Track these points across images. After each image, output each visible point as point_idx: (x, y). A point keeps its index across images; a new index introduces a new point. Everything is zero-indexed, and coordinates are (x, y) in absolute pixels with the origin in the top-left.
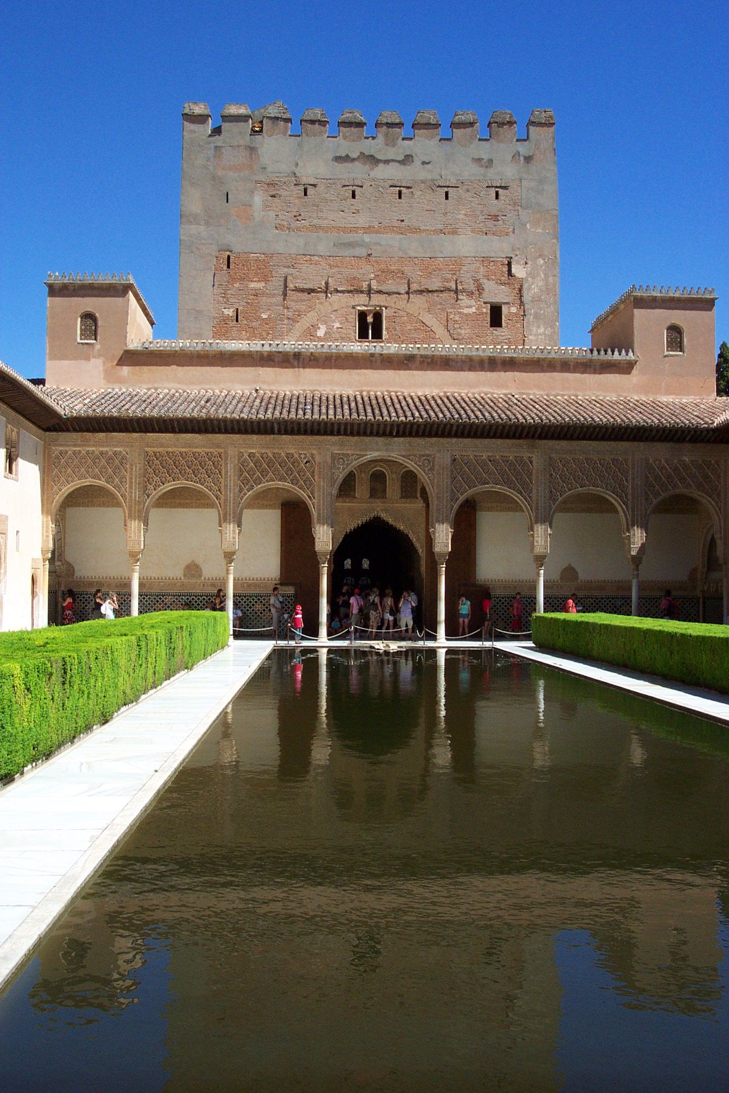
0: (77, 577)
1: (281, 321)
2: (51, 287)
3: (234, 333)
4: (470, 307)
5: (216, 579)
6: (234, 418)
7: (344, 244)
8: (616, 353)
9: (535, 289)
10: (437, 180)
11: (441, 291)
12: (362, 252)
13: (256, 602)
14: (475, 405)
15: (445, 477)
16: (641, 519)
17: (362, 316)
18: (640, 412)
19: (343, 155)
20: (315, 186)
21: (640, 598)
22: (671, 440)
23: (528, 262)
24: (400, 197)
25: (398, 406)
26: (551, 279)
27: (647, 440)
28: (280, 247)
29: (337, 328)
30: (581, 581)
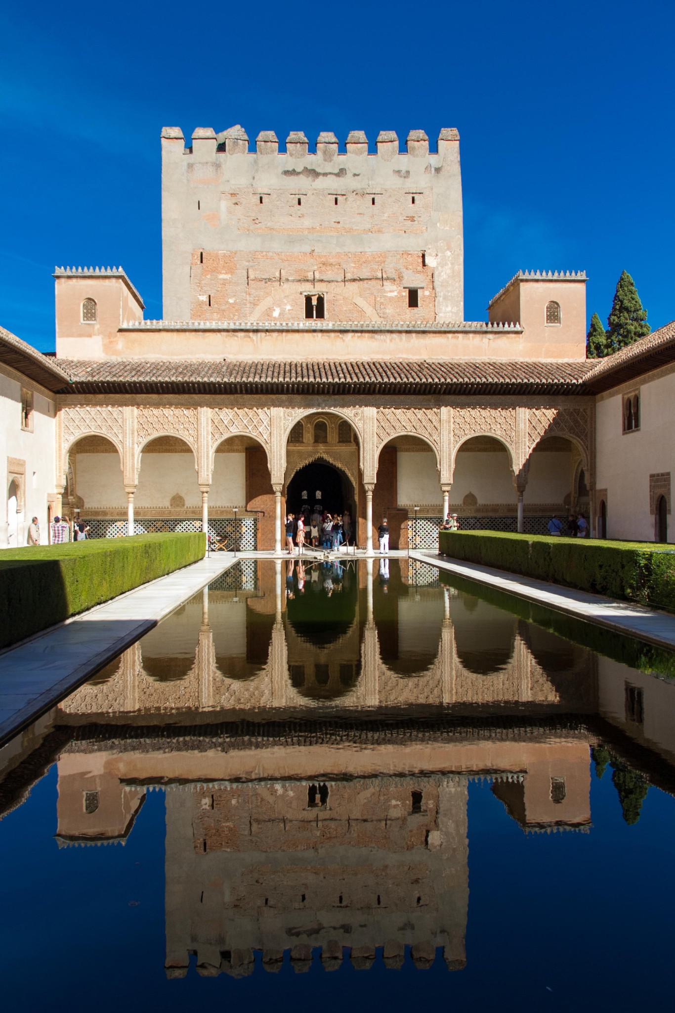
0: (86, 508)
5: (196, 507)
6: (205, 381)
8: (506, 325)
9: (444, 276)
10: (365, 189)
11: (370, 279)
12: (307, 249)
13: (227, 525)
14: (394, 369)
15: (371, 425)
17: (308, 299)
19: (291, 169)
23: (440, 255)
24: (336, 203)
25: (334, 371)
26: (457, 267)
27: (529, 393)
29: (289, 310)
30: (479, 505)
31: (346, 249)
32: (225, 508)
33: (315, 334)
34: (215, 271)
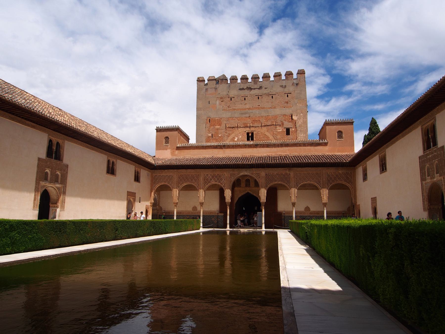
1: (225, 137)
2: (157, 130)
3: (211, 141)
4: (280, 129)
8: (321, 141)
10: (269, 93)
12: (248, 115)
13: (213, 218)
16: (326, 191)
17: (248, 134)
20: (234, 97)
21: (327, 216)
22: (335, 166)
24: (258, 99)
26: (305, 119)
30: (311, 211)
31: (262, 115)
32: (212, 211)
34: (214, 125)
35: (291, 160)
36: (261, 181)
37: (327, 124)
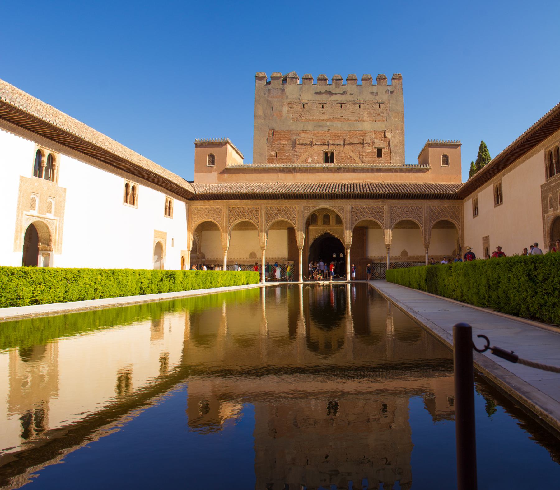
4: (369, 150)
7: (319, 126)
9: (395, 142)
12: (326, 129)
17: (326, 154)
18: (428, 188)
23: (393, 132)
24: (341, 107)
27: (430, 198)
28: (293, 127)
33: (324, 170)
35: (385, 189)
36: (346, 217)
37: (430, 145)
